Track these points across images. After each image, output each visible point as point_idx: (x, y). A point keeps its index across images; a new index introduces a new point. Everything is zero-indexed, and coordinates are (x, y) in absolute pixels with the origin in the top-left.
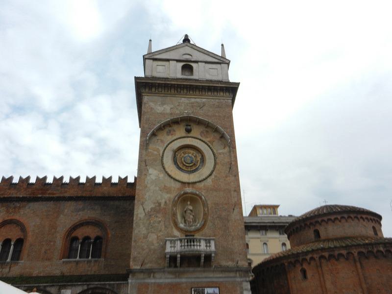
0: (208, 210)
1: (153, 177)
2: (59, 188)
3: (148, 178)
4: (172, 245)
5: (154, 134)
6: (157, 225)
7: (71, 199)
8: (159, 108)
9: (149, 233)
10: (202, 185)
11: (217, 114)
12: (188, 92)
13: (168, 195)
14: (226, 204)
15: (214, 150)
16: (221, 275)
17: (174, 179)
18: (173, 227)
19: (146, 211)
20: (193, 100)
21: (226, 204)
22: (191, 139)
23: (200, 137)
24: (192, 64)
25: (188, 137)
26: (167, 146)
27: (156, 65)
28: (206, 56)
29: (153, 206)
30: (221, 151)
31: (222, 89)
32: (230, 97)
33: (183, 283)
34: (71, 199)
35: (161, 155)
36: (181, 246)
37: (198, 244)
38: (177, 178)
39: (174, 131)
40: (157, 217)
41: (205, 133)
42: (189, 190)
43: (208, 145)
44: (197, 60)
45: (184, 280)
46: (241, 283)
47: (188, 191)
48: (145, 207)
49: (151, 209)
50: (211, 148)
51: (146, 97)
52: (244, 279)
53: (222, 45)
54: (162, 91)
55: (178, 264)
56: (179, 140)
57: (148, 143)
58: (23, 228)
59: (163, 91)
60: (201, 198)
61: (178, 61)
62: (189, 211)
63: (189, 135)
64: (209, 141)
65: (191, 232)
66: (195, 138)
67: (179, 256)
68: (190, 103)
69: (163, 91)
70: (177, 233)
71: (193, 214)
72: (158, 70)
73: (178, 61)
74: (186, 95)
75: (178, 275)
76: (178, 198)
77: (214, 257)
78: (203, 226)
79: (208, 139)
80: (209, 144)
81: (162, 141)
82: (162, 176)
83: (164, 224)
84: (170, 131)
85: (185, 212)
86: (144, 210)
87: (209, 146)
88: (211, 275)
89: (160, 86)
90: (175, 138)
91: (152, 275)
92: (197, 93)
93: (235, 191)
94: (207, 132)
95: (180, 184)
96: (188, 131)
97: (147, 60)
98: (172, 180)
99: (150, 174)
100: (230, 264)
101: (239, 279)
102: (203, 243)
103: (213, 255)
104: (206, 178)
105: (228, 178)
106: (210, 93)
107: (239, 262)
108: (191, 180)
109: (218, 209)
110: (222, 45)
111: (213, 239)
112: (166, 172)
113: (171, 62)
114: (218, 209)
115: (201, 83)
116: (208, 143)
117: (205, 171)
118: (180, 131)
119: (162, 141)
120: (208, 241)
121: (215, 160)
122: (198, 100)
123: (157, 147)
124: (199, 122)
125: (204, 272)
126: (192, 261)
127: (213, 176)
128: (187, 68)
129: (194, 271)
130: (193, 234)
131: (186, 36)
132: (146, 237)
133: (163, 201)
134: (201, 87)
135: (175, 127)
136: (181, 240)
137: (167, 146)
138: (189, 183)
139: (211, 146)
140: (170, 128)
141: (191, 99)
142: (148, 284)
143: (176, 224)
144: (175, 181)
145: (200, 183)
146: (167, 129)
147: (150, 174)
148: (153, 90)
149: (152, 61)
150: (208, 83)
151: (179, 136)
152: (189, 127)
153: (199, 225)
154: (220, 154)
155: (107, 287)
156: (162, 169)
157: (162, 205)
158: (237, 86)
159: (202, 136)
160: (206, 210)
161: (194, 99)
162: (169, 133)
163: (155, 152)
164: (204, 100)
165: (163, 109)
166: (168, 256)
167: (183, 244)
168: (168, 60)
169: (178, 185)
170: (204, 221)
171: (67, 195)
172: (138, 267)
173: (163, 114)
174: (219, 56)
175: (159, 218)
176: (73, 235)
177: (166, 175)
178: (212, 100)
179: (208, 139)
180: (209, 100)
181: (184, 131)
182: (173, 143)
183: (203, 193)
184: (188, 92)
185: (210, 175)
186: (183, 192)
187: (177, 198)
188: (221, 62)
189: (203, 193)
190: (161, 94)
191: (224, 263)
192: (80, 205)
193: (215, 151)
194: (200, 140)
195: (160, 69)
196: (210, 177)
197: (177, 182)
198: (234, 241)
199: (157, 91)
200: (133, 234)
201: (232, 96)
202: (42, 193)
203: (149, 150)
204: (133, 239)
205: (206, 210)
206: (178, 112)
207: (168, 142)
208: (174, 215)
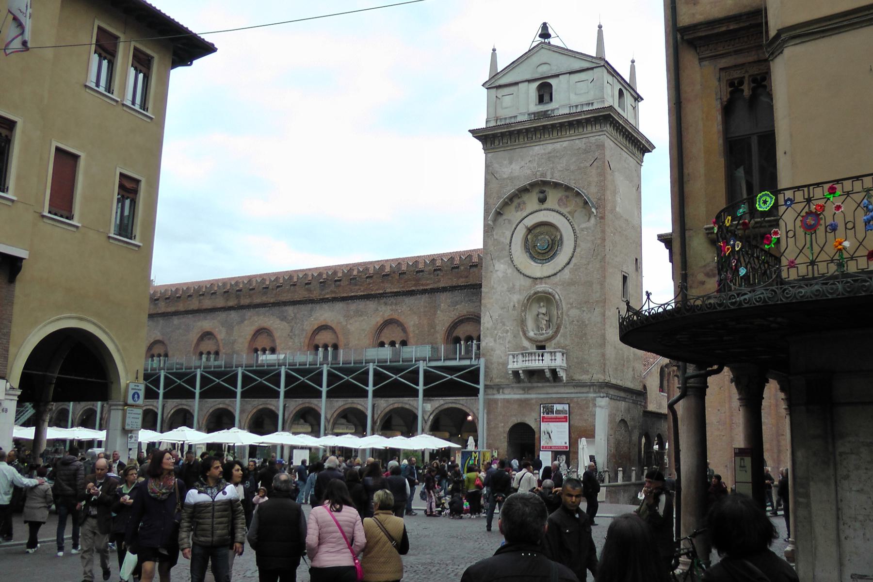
1: (500, 274)
2: (432, 276)
3: (495, 276)
5: (499, 214)
7: (444, 290)
8: (505, 170)
11: (582, 165)
14: (586, 303)
16: (572, 391)
19: (494, 318)
20: (550, 147)
21: (586, 303)
23: (557, 207)
24: (551, 81)
28: (572, 59)
30: (583, 226)
31: (588, 121)
33: (532, 399)
34: (444, 290)
39: (524, 203)
42: (541, 287)
44: (557, 72)
45: (533, 396)
46: (594, 399)
52: (598, 395)
53: (600, 27)
58: (404, 330)
61: (529, 81)
63: (543, 207)
64: (569, 213)
65: (541, 341)
68: (545, 154)
70: (526, 343)
72: (504, 105)
73: (529, 81)
75: (526, 390)
79: (569, 209)
80: (570, 217)
82: (510, 271)
84: (519, 204)
88: (562, 390)
89: (503, 134)
90: (525, 214)
92: (555, 134)
94: (567, 197)
95: (530, 280)
96: (542, 201)
100: (585, 378)
101: (592, 395)
104: (563, 269)
105: (590, 266)
106: (572, 132)
110: (600, 27)
115: (557, 119)
116: (567, 215)
117: (562, 258)
119: (510, 221)
121: (576, 241)
122: (558, 146)
123: (503, 233)
124: (556, 185)
125: (555, 387)
127: (571, 265)
128: (545, 92)
129: (543, 387)
130: (543, 344)
131: (545, 24)
133: (512, 304)
135: (526, 197)
138: (541, 278)
140: (519, 201)
142: (498, 400)
146: (516, 201)
148: (497, 142)
150: (567, 118)
152: (541, 195)
154: (582, 230)
155: (461, 402)
159: (559, 205)
160: (559, 313)
162: (518, 208)
163: (502, 239)
164: (565, 144)
168: (516, 84)
171: (441, 285)
173: (511, 179)
176: (454, 335)
178: (577, 141)
179: (569, 209)
183: (559, 293)
185: (568, 263)
188: (595, 65)
189: (558, 290)
192: (458, 296)
195: (507, 101)
198: (592, 350)
202: (415, 285)
203: (495, 237)
205: (559, 313)
206: (529, 172)
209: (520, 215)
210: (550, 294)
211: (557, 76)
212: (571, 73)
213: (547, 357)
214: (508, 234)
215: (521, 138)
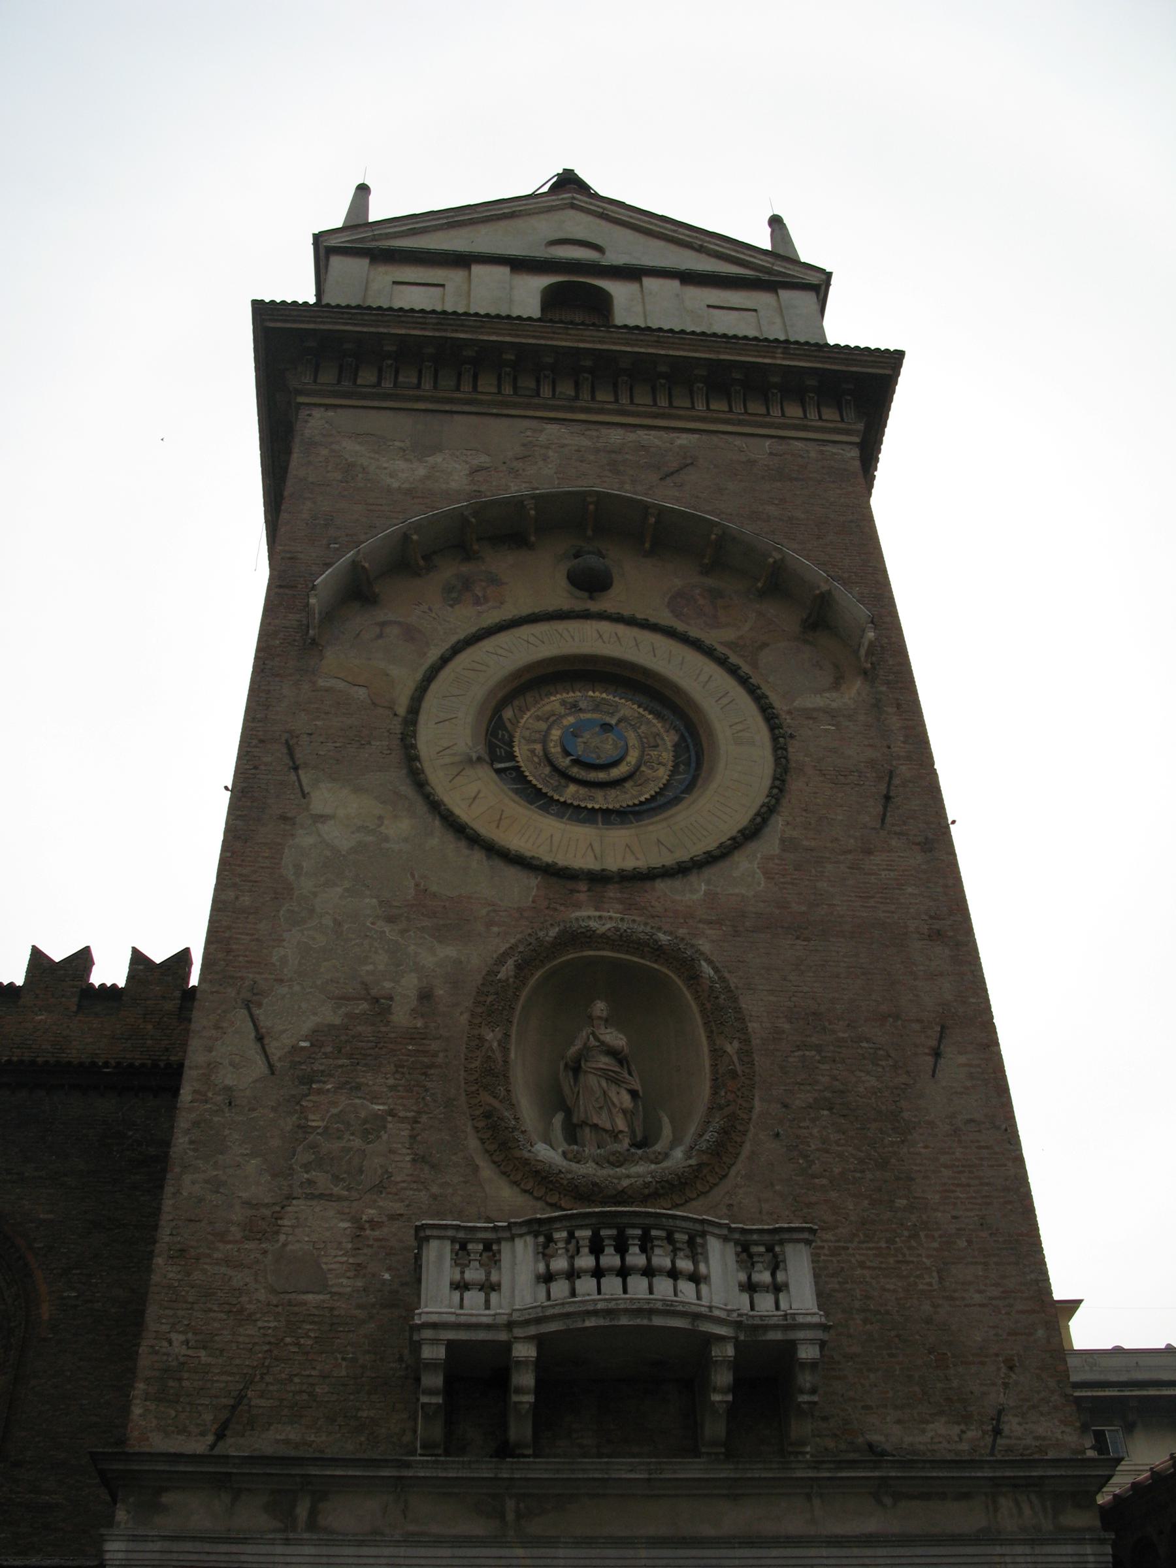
0: (746, 1053)
3: (306, 840)
4: (474, 1274)
5: (359, 591)
6: (357, 1143)
8: (401, 464)
9: (290, 1197)
10: (692, 893)
12: (585, 395)
13: (449, 951)
15: (765, 689)
17: (493, 850)
18: (482, 1162)
19: (276, 1049)
20: (616, 436)
22: (605, 627)
23: (665, 618)
25: (586, 615)
26: (445, 660)
27: (389, 279)
29: (330, 1016)
32: (847, 432)
35: (402, 711)
36: (548, 1278)
37: (684, 1265)
38: (516, 842)
39: (494, 580)
40: (358, 1087)
41: (701, 602)
43: (722, 662)
47: (593, 924)
48: (265, 1022)
49: (317, 1037)
50: (744, 681)
51: (317, 413)
54: (418, 386)
55: (520, 1431)
56: (525, 631)
57: (314, 642)
59: (427, 385)
60: (693, 977)
61: (519, 265)
62: (604, 1061)
66: (631, 622)
67: (525, 1351)
69: (427, 385)
71: (637, 1086)
73: (519, 265)
74: (572, 409)
76: (519, 967)
77: (813, 1365)
78: (720, 1152)
80: (734, 659)
81: (410, 634)
83: (413, 1137)
84: (467, 584)
85: (576, 1069)
86: (260, 1039)
87: (733, 671)
91: (302, 1511)
93: (936, 936)
95: (533, 882)
97: (336, 261)
98: (478, 855)
99: (323, 818)
100: (939, 1436)
102: (719, 1260)
103: (807, 1353)
106: (719, 405)
107: (1012, 1425)
108: (614, 862)
109: (818, 1048)
111: (807, 1236)
112: (435, 806)
113: (476, 269)
114: (818, 1048)
118: (537, 580)
119: (410, 634)
120: (759, 1250)
123: (368, 664)
126: (619, 1395)
127: (769, 844)
132: (263, 1226)
133: (410, 984)
134: (663, 369)
135: (501, 562)
136: (540, 1229)
137: (445, 660)
139: (746, 668)
140: (465, 569)
141: (604, 431)
143: (502, 1142)
144: (499, 864)
145: (677, 883)
146: (449, 571)
147: (323, 818)
149: (366, 262)
151: (525, 611)
153: (678, 1153)
154: (809, 715)
156: (407, 790)
157: (401, 1016)
158: (887, 372)
160: (731, 1048)
161: (620, 431)
164: (683, 440)
165: (422, 471)
166: (433, 1353)
167: (560, 1264)
169: (520, 889)
170: (717, 1122)
172: (198, 1446)
174: (765, 252)
175: (374, 1098)
177: (437, 823)
178: (738, 442)
179: (729, 635)
180: (715, 439)
181: (564, 582)
182: (488, 644)
184: (585, 395)
185: (751, 833)
186: (553, 932)
187: (507, 970)
189: (706, 947)
190: (418, 399)
191: (888, 1432)
193: (775, 700)
194: (670, 633)
196: (752, 846)
197: (512, 873)
199: (387, 384)
200: (168, 1204)
201: (860, 426)
204: (164, 1235)
205: (731, 1048)
207: (453, 639)
208: (491, 1076)
209: (464, 619)
210: (657, 951)
211: (632, 274)
212: (688, 278)
213: (719, 1260)
214: (405, 681)
215: (487, 384)
